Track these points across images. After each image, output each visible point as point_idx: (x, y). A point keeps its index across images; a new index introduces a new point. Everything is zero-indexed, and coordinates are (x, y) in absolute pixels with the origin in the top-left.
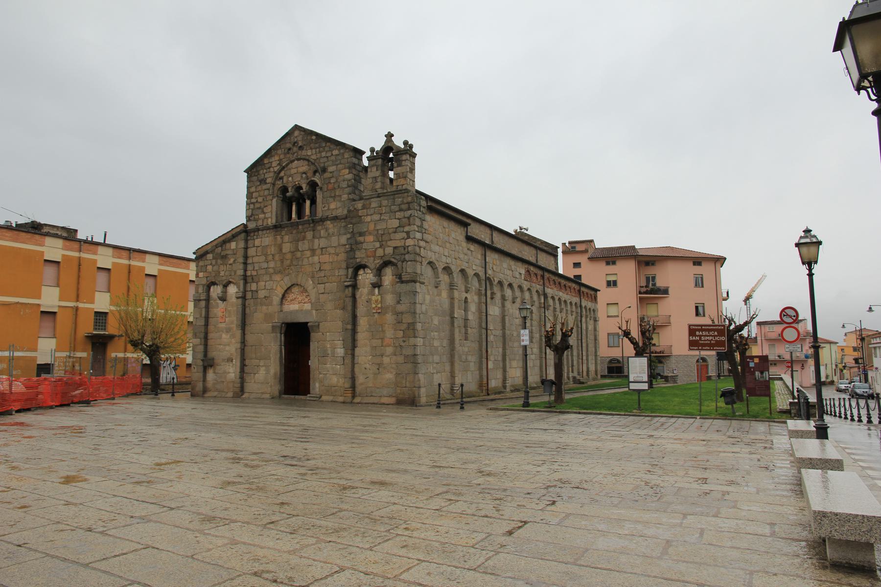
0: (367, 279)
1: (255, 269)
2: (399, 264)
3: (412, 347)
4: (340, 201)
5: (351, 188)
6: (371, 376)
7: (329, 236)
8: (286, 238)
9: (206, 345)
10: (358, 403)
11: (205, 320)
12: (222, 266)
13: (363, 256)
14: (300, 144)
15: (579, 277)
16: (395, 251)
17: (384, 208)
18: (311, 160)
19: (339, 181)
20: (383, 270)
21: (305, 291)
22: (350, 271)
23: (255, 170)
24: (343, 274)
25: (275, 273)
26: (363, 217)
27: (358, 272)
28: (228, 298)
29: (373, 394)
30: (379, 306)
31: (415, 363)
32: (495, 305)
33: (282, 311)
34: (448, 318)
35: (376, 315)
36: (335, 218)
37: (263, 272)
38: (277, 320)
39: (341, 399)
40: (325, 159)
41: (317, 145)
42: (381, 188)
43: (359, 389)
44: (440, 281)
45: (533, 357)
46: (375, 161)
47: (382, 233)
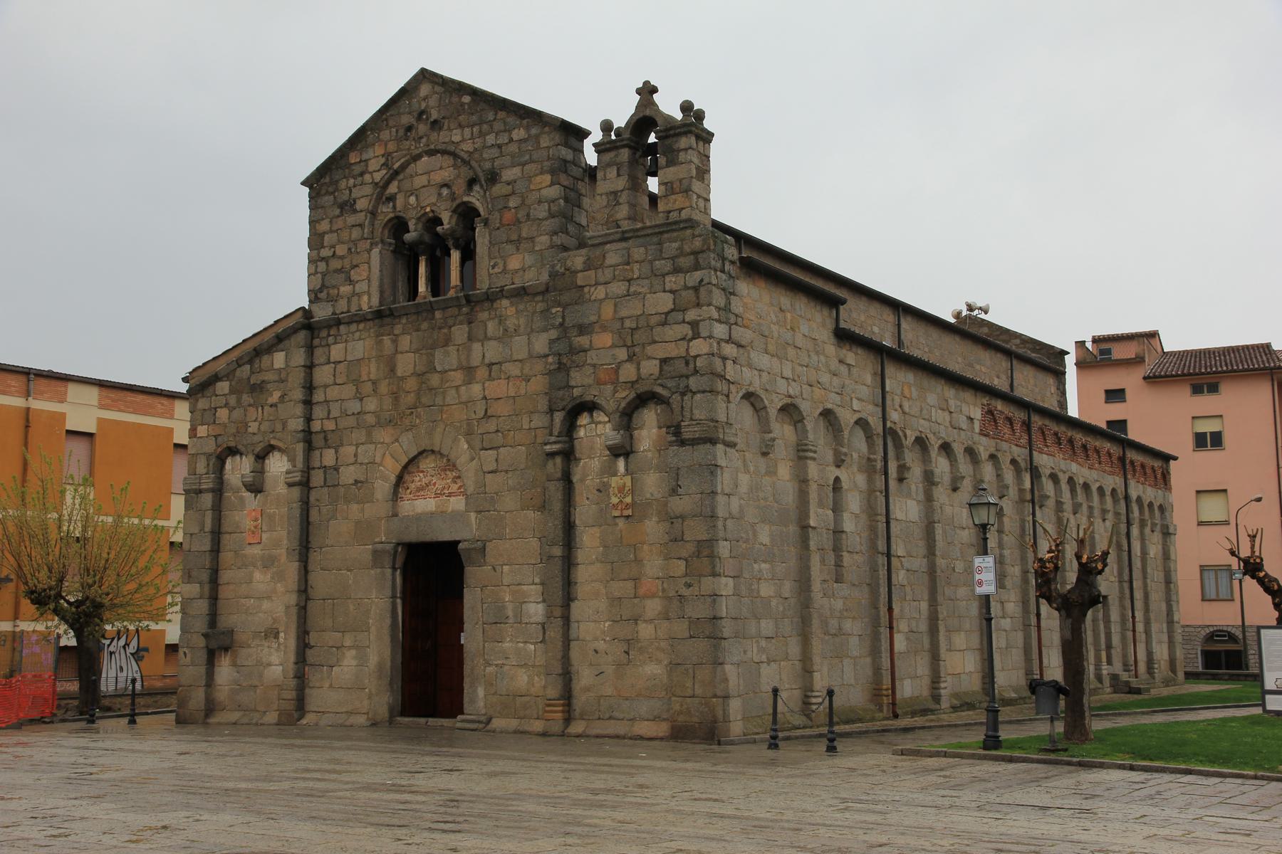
0: (599, 436)
1: (331, 416)
3: (709, 600)
4: (532, 251)
5: (556, 220)
6: (610, 670)
7: (505, 336)
8: (405, 341)
9: (214, 598)
10: (578, 736)
11: (213, 540)
12: (252, 410)
13: (590, 381)
14: (435, 115)
15: (1121, 425)
16: (665, 368)
17: (636, 267)
18: (462, 154)
19: (528, 202)
20: (635, 415)
21: (450, 465)
22: (559, 417)
23: (327, 180)
24: (540, 424)
25: (379, 424)
26: (586, 290)
27: (576, 421)
28: (268, 485)
29: (616, 714)
30: (628, 500)
31: (716, 639)
32: (909, 495)
33: (395, 515)
34: (793, 529)
35: (621, 522)
36: (521, 293)
37: (351, 421)
38: (385, 536)
39: (538, 726)
40: (495, 152)
41: (474, 118)
42: (629, 219)
43: (580, 701)
44: (774, 440)
45: (1006, 623)
46: (612, 154)
47: (634, 325)
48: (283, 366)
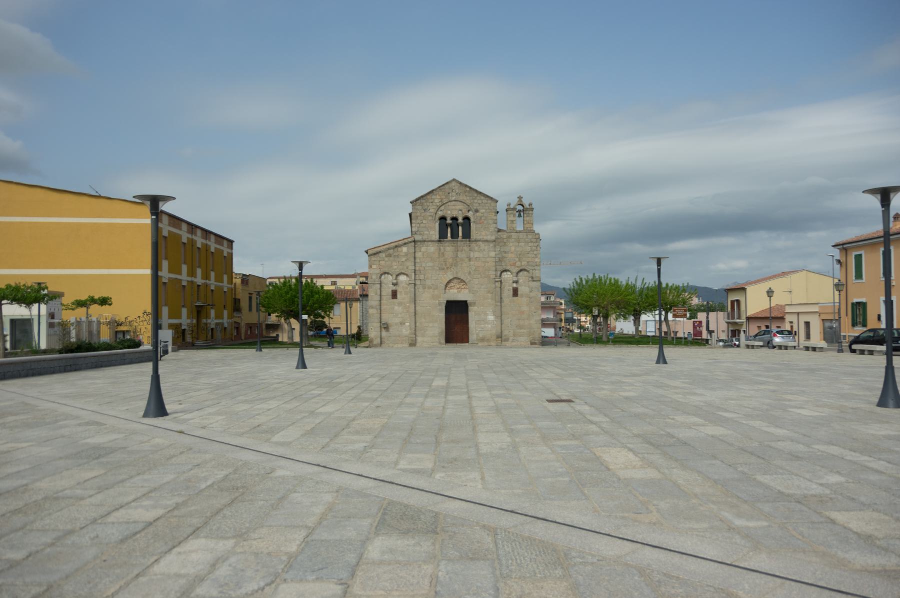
2: (531, 271)
8: (448, 249)
14: (457, 191)
22: (499, 273)
40: (477, 205)
46: (512, 211)
48: (406, 251)
